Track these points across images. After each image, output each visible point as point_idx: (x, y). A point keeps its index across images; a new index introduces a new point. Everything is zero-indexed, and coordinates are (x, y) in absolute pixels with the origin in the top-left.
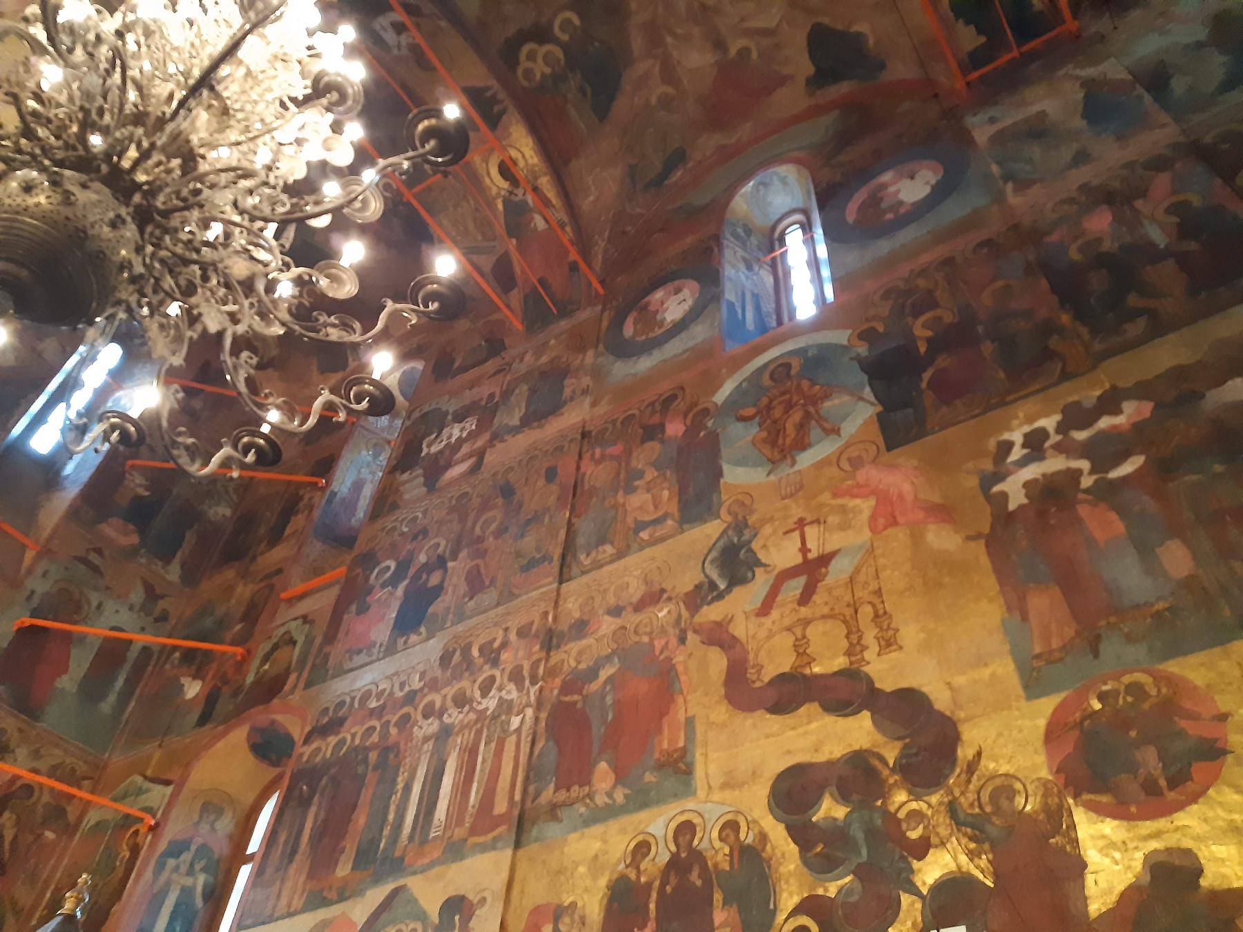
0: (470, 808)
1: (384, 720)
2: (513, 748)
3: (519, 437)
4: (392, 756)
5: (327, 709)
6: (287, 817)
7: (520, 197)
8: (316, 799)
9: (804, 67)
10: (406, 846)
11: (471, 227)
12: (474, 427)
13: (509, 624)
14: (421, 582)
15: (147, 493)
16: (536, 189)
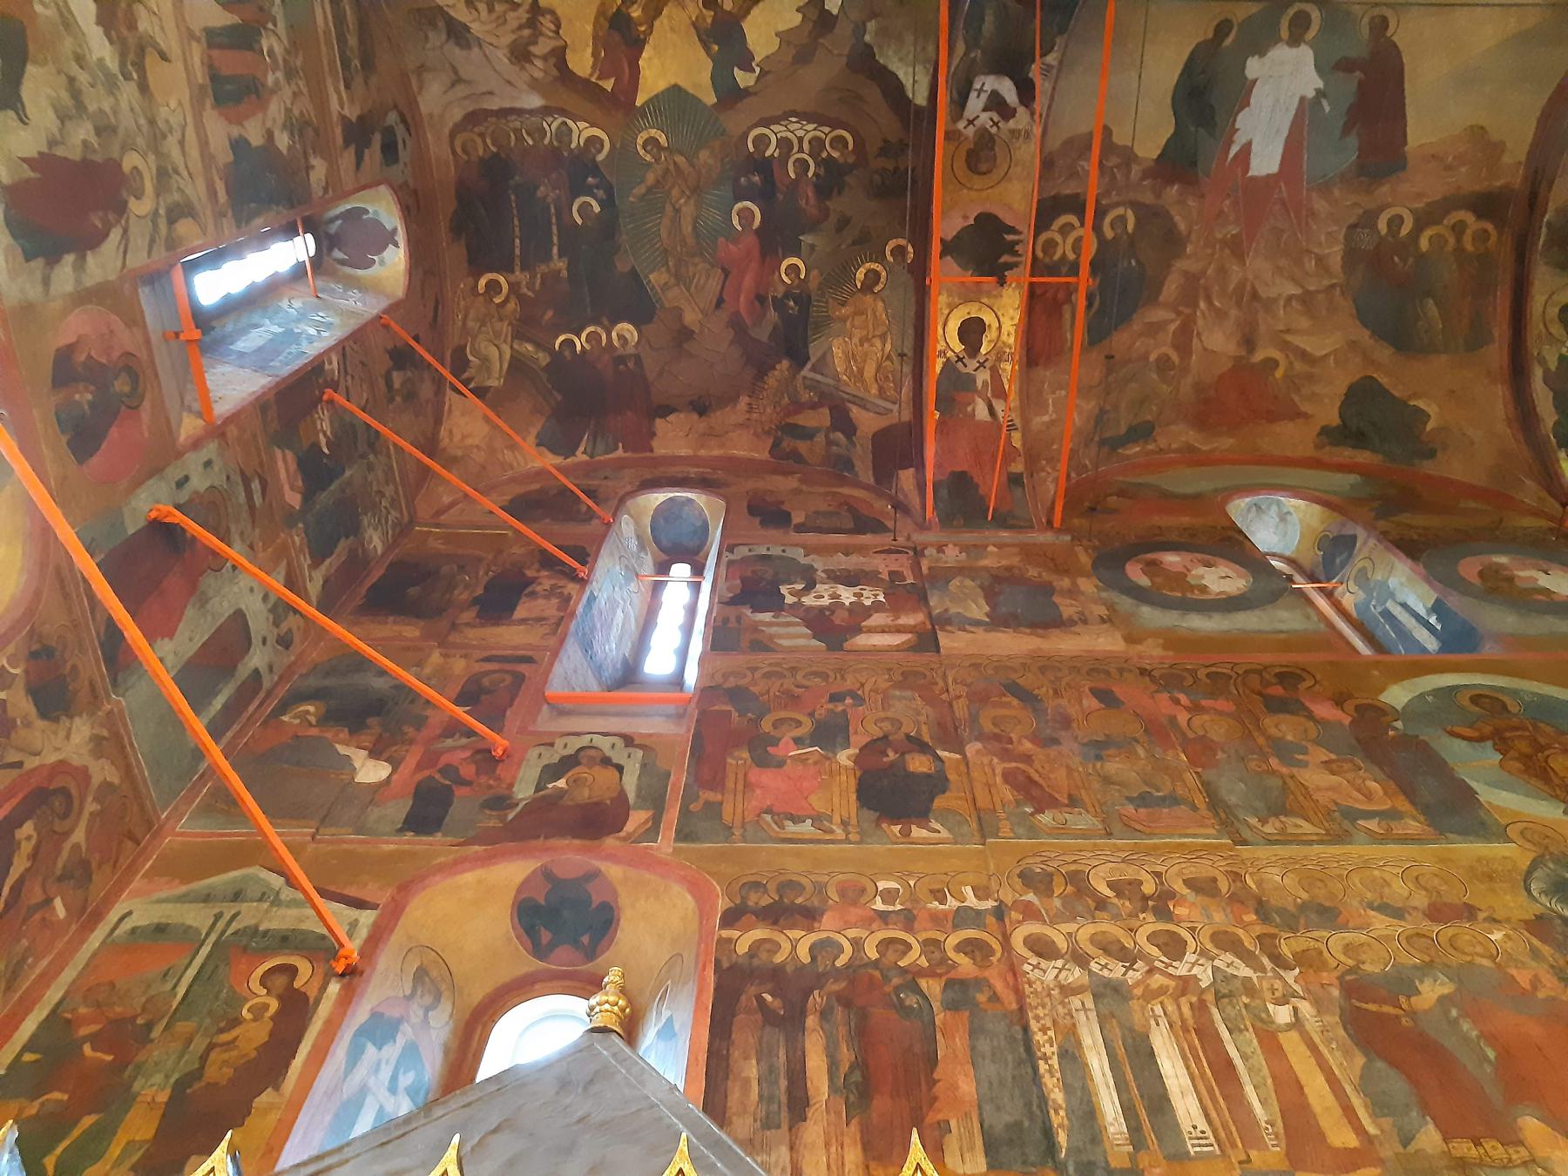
0: (1264, 1125)
1: (923, 936)
2: (1303, 1048)
3: (1000, 635)
4: (982, 998)
5: (756, 885)
6: (745, 1035)
7: (970, 369)
8: (811, 1021)
9: (1330, 415)
10: (1132, 1157)
11: (870, 371)
12: (881, 598)
13: (1158, 868)
14: (885, 759)
15: (326, 451)
16: (995, 374)
